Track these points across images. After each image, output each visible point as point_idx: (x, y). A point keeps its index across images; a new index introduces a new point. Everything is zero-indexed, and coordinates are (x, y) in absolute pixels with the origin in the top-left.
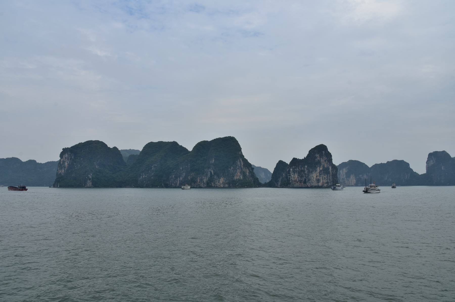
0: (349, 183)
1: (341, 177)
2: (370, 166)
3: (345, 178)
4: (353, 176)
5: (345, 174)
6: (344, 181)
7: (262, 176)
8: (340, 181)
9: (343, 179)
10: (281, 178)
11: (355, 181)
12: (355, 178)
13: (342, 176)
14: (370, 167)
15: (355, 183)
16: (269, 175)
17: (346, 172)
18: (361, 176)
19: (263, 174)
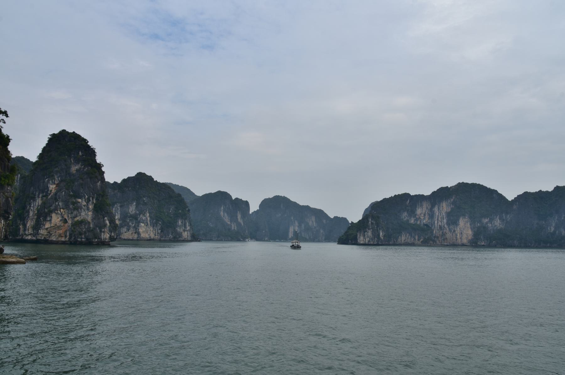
0: (456, 238)
1: (436, 222)
2: (510, 197)
3: (446, 226)
4: (466, 220)
5: (444, 217)
6: (442, 233)
7: (310, 223)
8: (434, 232)
9: (440, 227)
10: (39, 201)
11: (470, 232)
12: (470, 225)
13: (438, 219)
14: (510, 199)
15: (470, 238)
16: (324, 221)
17: (449, 210)
18: (485, 220)
19: (313, 219)
